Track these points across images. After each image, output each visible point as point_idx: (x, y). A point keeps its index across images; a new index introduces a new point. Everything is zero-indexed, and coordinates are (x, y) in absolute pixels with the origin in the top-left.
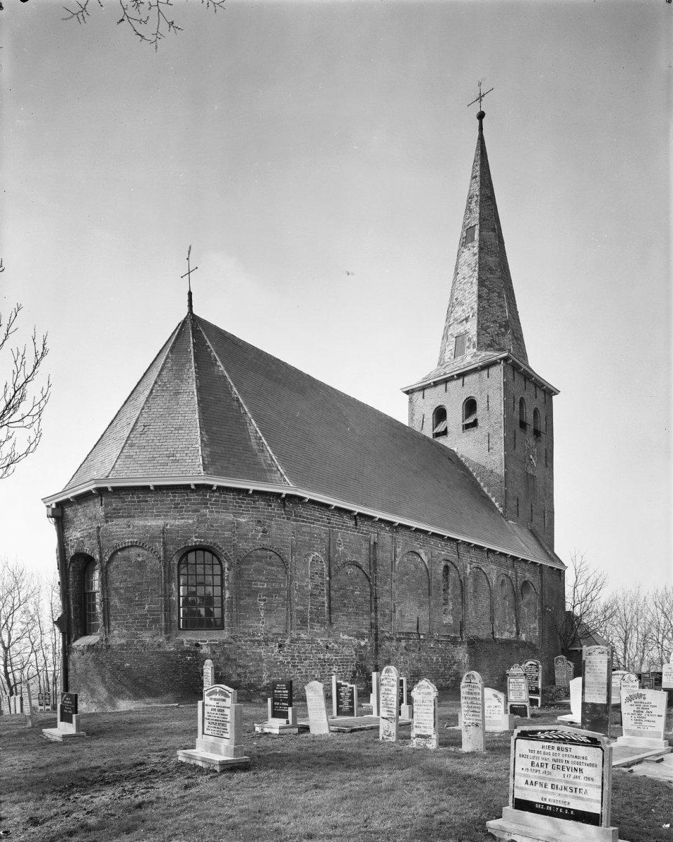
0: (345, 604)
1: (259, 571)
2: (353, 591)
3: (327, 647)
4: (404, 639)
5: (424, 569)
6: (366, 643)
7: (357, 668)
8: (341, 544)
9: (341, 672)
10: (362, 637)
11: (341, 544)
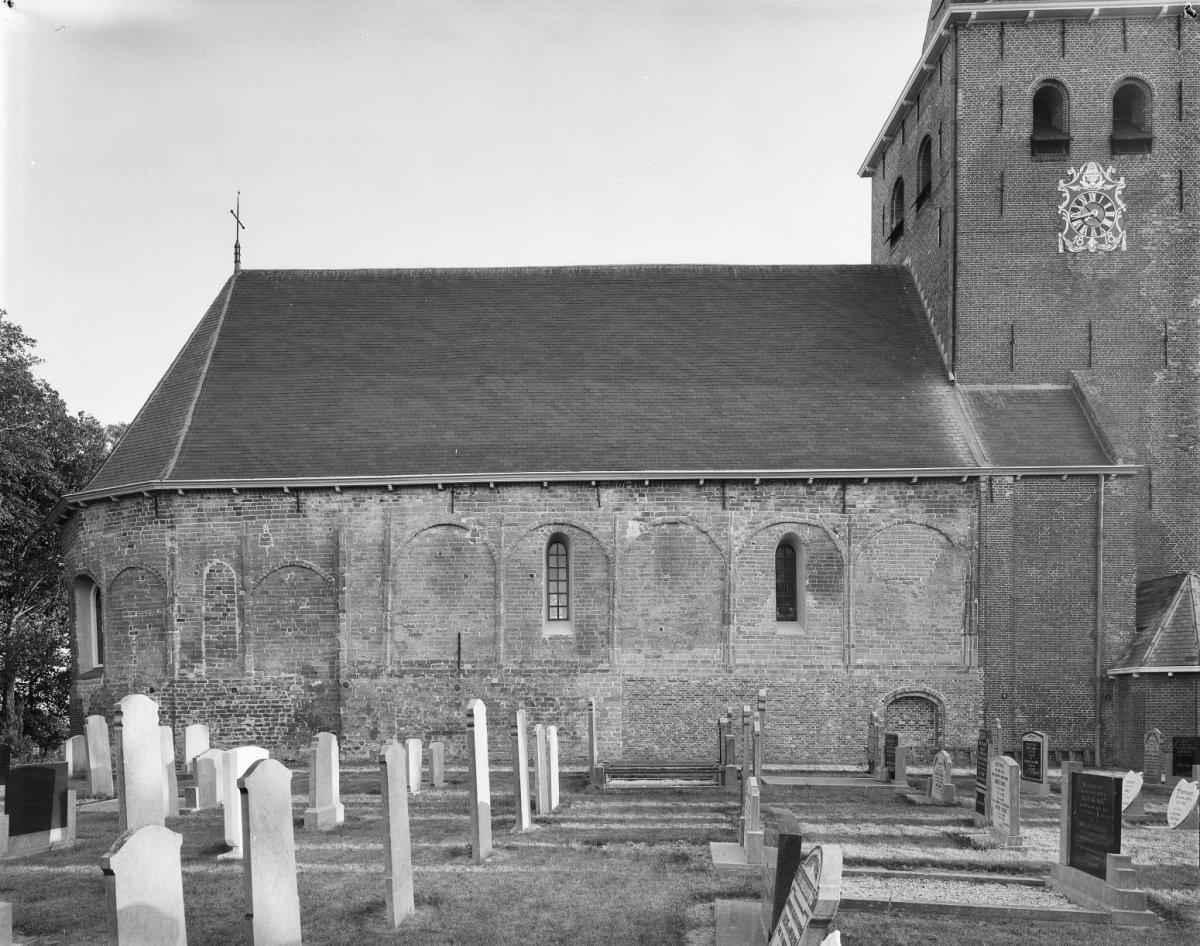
1: (129, 597)
2: (295, 607)
3: (234, 690)
9: (261, 725)
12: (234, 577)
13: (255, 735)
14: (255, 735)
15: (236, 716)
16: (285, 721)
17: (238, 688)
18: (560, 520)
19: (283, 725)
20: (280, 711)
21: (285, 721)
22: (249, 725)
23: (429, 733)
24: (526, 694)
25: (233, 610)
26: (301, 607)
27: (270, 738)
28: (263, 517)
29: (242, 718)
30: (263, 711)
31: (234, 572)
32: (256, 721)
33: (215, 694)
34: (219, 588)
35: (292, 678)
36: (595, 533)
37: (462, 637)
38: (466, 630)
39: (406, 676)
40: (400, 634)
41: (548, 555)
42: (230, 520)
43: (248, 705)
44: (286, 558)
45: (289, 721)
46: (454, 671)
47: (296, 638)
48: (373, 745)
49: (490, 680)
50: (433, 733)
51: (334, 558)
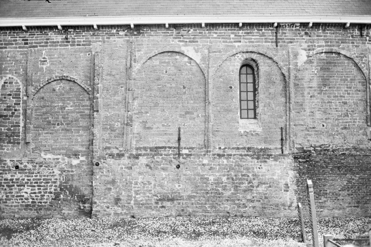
0: (49, 122)
2: (63, 108)
3: (17, 167)
4: (144, 155)
5: (195, 68)
6: (82, 161)
7: (61, 189)
8: (46, 61)
9: (35, 193)
10: (76, 155)
11: (46, 61)
12: (21, 87)
13: (31, 200)
14: (31, 200)
15: (18, 186)
16: (53, 190)
17: (20, 166)
18: (250, 49)
19: (51, 193)
20: (48, 183)
21: (53, 190)
22: (26, 193)
23: (158, 200)
24: (228, 172)
25: (19, 110)
26: (66, 108)
27: (41, 203)
28: (43, 46)
29: (22, 188)
30: (37, 183)
31: (20, 83)
32: (32, 190)
33: (3, 170)
34: (10, 95)
35: (58, 159)
36: (275, 58)
37: (182, 130)
38: (184, 125)
39: (140, 157)
40: (137, 127)
41: (240, 74)
42: (20, 48)
43: (26, 178)
44: (57, 74)
45: (55, 190)
46: (176, 154)
47: (63, 130)
48: (116, 207)
49: (202, 162)
50: (160, 200)
51: (93, 73)
